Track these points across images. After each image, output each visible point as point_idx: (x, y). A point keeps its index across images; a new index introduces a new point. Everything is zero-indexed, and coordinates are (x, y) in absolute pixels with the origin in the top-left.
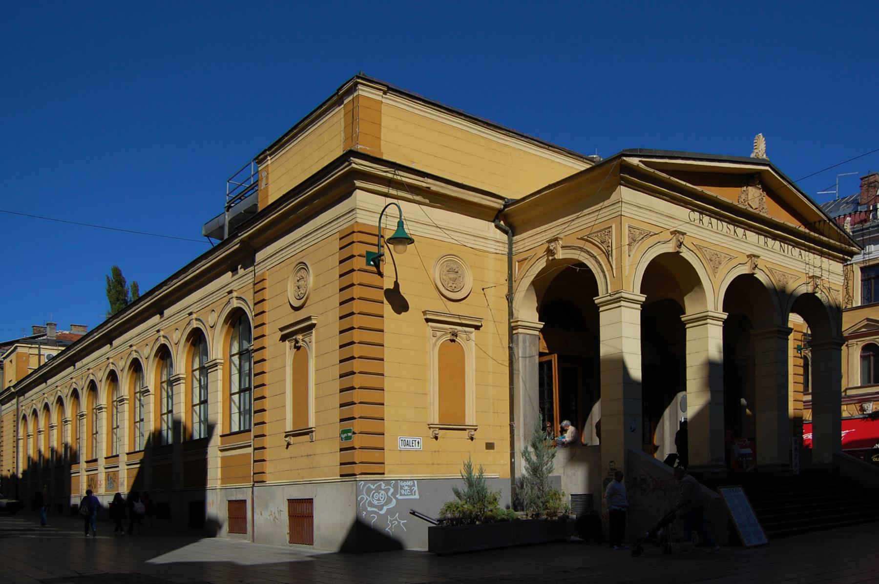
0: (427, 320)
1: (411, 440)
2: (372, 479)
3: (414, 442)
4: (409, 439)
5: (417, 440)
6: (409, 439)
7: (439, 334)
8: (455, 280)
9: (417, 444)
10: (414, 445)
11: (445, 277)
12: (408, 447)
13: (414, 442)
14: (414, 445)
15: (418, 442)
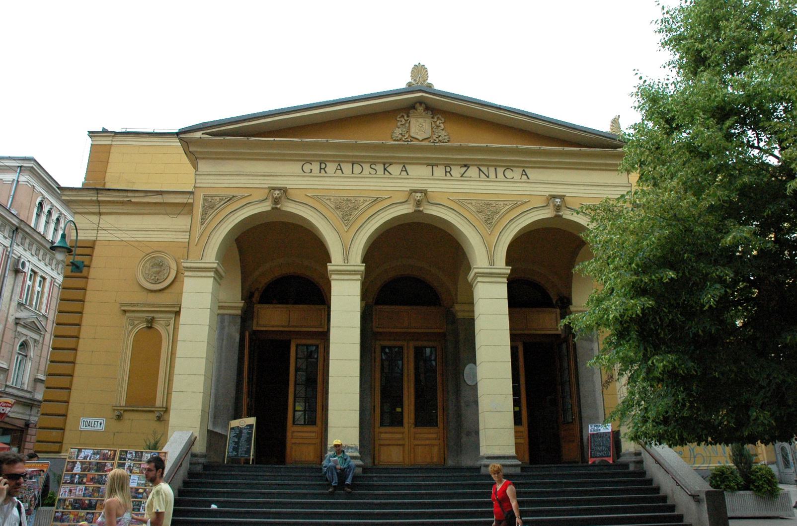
0: (125, 311)
1: (93, 421)
2: (47, 457)
3: (96, 423)
4: (91, 420)
5: (100, 421)
6: (91, 420)
7: (136, 322)
8: (158, 273)
9: (99, 425)
10: (95, 426)
11: (147, 272)
12: (89, 428)
13: (96, 423)
14: (95, 426)
15: (101, 424)
